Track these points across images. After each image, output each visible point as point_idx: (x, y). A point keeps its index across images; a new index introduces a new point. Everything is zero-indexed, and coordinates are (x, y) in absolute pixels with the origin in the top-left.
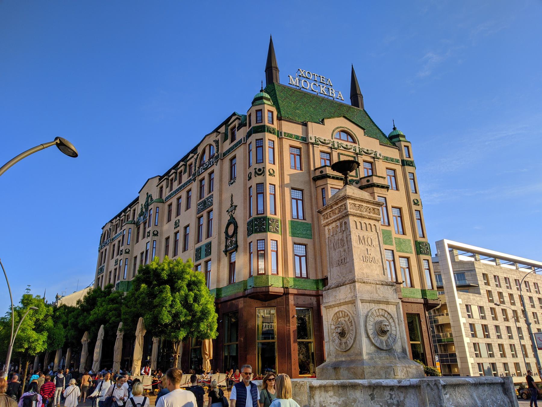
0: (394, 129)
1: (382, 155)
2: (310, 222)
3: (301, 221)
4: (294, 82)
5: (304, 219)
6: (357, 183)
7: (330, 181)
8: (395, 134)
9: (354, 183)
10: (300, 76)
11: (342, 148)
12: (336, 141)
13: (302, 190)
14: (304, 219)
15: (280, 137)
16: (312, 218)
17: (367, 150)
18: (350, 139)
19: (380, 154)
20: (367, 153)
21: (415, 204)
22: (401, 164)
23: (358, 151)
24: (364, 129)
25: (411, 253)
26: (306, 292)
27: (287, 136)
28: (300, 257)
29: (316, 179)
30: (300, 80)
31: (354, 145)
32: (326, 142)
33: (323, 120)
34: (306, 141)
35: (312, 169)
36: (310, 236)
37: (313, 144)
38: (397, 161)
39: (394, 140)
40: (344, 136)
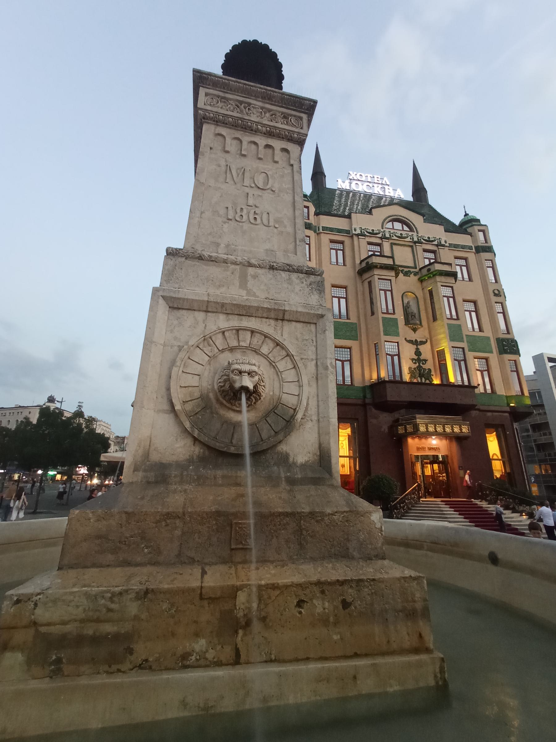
0: (466, 215)
1: (448, 243)
2: (355, 322)
3: (344, 321)
4: (346, 186)
5: (348, 318)
6: (415, 275)
7: (377, 272)
8: (466, 219)
9: (412, 275)
10: (351, 179)
11: (395, 238)
12: (387, 230)
13: (345, 288)
14: (348, 318)
15: (318, 232)
16: (359, 317)
17: (429, 238)
18: (406, 228)
19: (446, 242)
20: (429, 241)
21: (495, 295)
22: (474, 250)
23: (416, 239)
24: (423, 215)
25: (491, 352)
26: (349, 401)
27: (326, 230)
28: (343, 362)
29: (361, 272)
30: (350, 183)
31: (410, 233)
32: (375, 232)
33: (371, 210)
34: (349, 234)
35: (358, 262)
36: (355, 338)
37: (358, 235)
38: (470, 248)
39: (465, 227)
40: (398, 226)
